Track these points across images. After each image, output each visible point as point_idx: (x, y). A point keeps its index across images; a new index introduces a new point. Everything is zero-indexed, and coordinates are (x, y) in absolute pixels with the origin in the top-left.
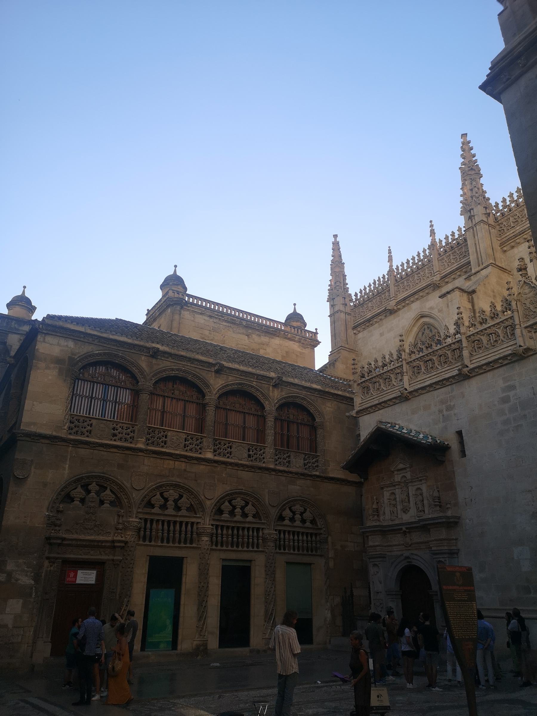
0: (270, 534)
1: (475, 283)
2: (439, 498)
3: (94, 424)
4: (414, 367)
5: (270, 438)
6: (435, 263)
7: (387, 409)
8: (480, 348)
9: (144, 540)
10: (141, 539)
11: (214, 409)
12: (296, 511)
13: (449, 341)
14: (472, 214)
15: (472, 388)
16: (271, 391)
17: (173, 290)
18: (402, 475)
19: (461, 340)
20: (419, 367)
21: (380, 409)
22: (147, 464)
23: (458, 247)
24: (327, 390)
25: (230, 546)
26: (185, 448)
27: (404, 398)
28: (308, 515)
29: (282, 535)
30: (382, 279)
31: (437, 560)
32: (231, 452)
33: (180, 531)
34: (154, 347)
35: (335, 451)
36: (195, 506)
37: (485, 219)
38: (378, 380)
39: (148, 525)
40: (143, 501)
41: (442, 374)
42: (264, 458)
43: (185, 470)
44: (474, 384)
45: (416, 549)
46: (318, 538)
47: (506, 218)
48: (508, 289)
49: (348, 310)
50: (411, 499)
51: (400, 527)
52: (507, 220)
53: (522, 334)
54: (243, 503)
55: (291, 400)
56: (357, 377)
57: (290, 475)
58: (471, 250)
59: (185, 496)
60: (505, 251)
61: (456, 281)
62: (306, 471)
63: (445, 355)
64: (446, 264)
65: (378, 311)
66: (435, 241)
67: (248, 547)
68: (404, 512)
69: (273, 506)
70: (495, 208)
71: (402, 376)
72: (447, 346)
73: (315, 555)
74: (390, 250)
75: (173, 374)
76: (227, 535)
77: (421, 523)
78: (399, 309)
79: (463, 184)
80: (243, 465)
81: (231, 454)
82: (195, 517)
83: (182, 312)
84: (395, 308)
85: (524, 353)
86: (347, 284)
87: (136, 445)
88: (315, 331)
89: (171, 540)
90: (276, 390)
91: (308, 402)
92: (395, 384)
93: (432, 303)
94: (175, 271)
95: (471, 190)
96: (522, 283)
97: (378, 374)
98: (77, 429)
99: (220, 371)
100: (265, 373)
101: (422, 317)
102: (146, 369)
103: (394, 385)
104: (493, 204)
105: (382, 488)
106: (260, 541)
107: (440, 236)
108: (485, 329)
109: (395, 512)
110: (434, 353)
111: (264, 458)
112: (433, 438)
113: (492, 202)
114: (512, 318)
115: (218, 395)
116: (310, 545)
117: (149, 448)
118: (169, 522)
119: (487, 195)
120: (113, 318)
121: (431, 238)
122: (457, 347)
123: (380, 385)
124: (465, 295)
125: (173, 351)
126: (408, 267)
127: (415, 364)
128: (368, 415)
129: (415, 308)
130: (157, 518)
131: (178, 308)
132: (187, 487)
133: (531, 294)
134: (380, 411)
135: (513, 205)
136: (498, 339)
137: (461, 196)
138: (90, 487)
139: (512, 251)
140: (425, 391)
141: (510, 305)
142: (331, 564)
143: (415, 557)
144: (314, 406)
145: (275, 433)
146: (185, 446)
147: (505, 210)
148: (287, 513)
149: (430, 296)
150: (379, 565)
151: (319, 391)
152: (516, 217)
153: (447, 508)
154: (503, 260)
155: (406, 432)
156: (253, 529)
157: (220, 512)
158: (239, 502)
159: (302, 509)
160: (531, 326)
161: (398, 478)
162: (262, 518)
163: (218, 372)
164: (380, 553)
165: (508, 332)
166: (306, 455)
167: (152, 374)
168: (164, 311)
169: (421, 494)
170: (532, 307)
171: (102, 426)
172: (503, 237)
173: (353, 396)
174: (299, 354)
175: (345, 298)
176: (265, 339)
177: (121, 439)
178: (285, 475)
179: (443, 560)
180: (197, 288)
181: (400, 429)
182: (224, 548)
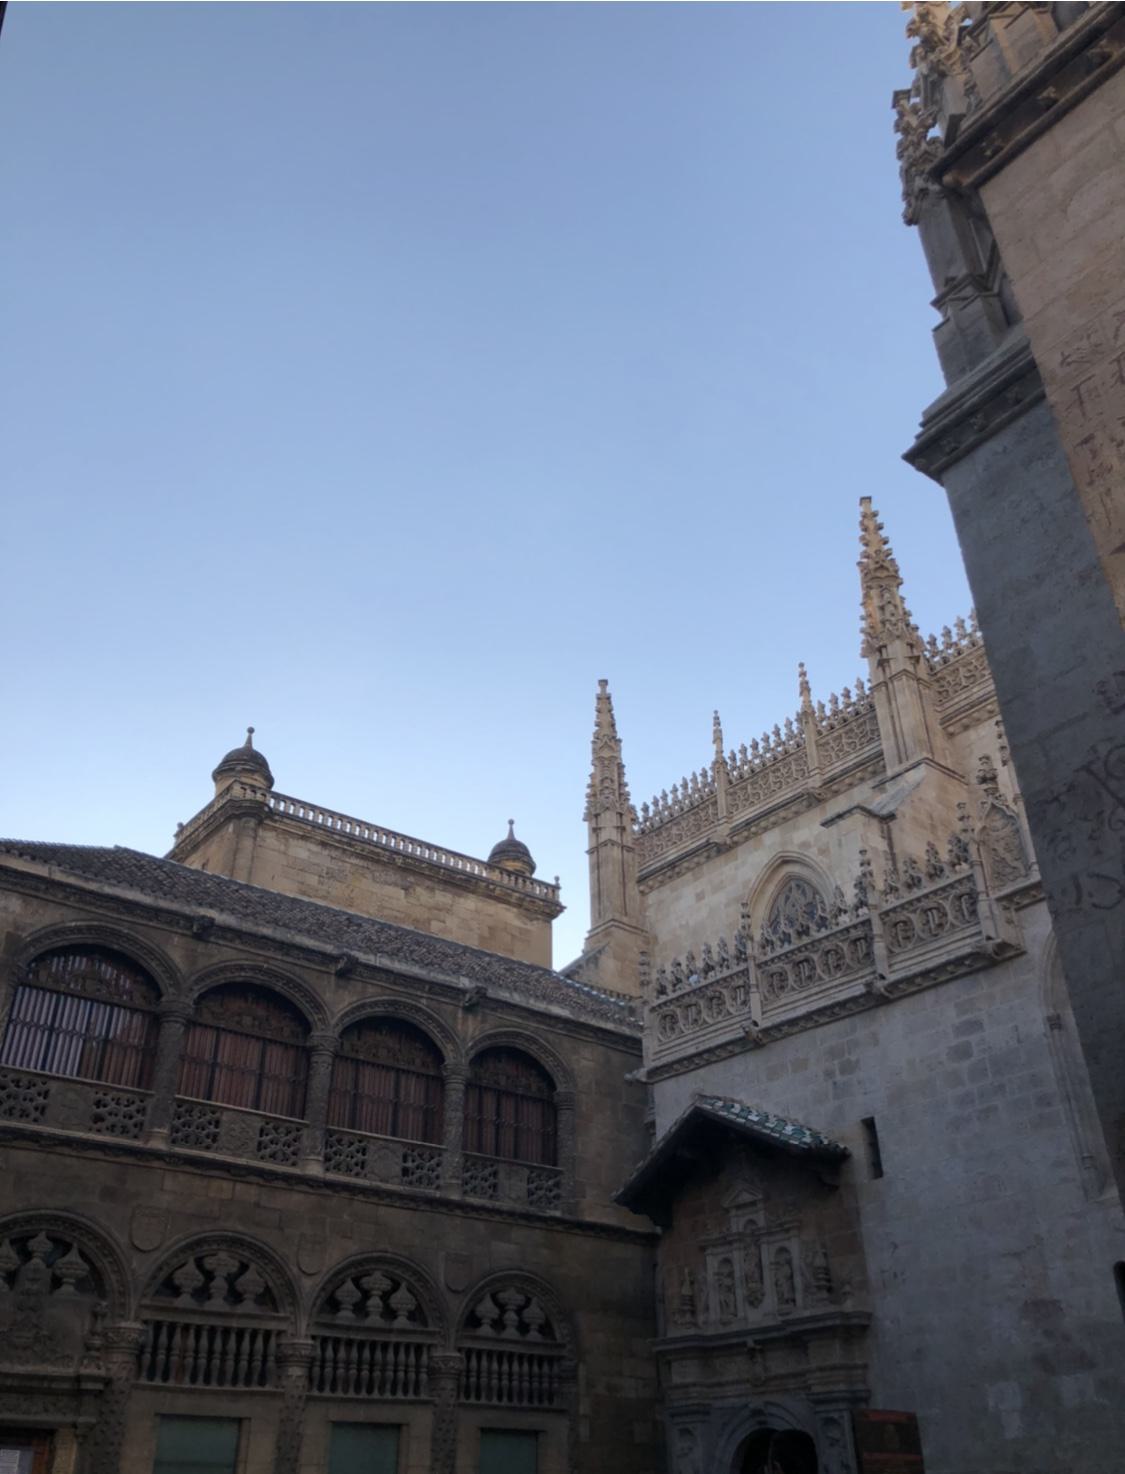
0: (446, 1360)
1: (893, 797)
2: (827, 1270)
3: (52, 1091)
4: (772, 976)
5: (453, 1131)
6: (812, 750)
9: (151, 1377)
10: (144, 1374)
11: (330, 1061)
12: (506, 1304)
13: (845, 920)
14: (885, 656)
15: (893, 1022)
16: (460, 1021)
17: (242, 783)
20: (782, 975)
21: (699, 1067)
22: (170, 1190)
23: (856, 721)
24: (582, 1020)
25: (352, 1390)
26: (259, 1150)
27: (751, 1043)
28: (534, 1313)
29: (474, 1363)
30: (700, 779)
32: (363, 1163)
33: (238, 1354)
34: (203, 917)
35: (599, 1161)
36: (275, 1292)
37: (910, 668)
38: (694, 1000)
39: (163, 1339)
40: (154, 1277)
41: (832, 991)
42: (438, 1177)
43: (257, 1205)
46: (556, 1369)
47: (951, 668)
48: (961, 819)
49: (628, 840)
50: (767, 1274)
51: (741, 1340)
52: (954, 671)
53: (992, 912)
54: (386, 1284)
55: (503, 1041)
56: (649, 994)
57: (497, 1218)
58: (885, 727)
59: (253, 1266)
60: (951, 735)
61: (856, 790)
62: (532, 1210)
63: (837, 951)
64: (833, 754)
65: (693, 846)
66: (810, 706)
67: (394, 1392)
68: (751, 1303)
69: (454, 1292)
70: (928, 647)
71: (747, 993)
72: (841, 931)
73: (547, 1411)
74: (717, 718)
75: (241, 976)
76: (348, 1363)
77: (790, 1329)
78: (736, 844)
79: (866, 596)
80: (390, 1194)
81: (362, 1168)
82: (274, 1318)
83: (261, 832)
84: (728, 841)
85: (997, 954)
86: (626, 785)
87: (147, 1141)
88: (553, 882)
89: (215, 1374)
90: (470, 1017)
91: (542, 1047)
92: (732, 1010)
93: (807, 832)
94: (249, 741)
95: (882, 608)
96: (988, 807)
97: (695, 986)
98: (12, 1102)
99: (349, 971)
100: (448, 978)
101: (786, 862)
102: (181, 966)
103: (729, 1013)
104: (926, 639)
105: (703, 1249)
106: (424, 1377)
107: (820, 696)
108: (918, 900)
110: (813, 946)
111: (438, 1177)
112: (815, 1135)
113: (924, 634)
114: (970, 878)
115: (340, 1028)
116: (536, 1385)
117: (178, 1150)
118: (212, 1330)
119: (913, 621)
120: (109, 844)
121: (802, 699)
122: (862, 937)
123: (699, 1012)
124: (875, 823)
125: (247, 926)
126: (755, 756)
127: (774, 968)
128: (674, 1079)
129: (772, 842)
130: (182, 1320)
131: (252, 823)
132: (260, 1245)
134: (701, 1072)
135: (964, 642)
136: (943, 920)
137: (862, 618)
138: (32, 1244)
139: (965, 734)
140: (796, 1029)
141: (966, 850)
142: (584, 1431)
143: (774, 1410)
144: (553, 1055)
145: (466, 1118)
146: (260, 1146)
147: (950, 651)
148: (487, 1309)
149: (801, 819)
151: (566, 1021)
152: (971, 667)
153: (845, 1294)
154: (947, 752)
155: (756, 1119)
156: (408, 1347)
157: (333, 1304)
158: (377, 1282)
159: (520, 1299)
160: (1009, 897)
161: (737, 1224)
162: (430, 1321)
163: (343, 975)
164: (696, 1402)
165: (964, 906)
166: (532, 1169)
167: (193, 978)
168: (218, 829)
169: (789, 1262)
170: (1008, 857)
171: (71, 1095)
172: (948, 705)
173: (640, 1035)
174: (517, 934)
175: (621, 815)
176: (442, 897)
177: (112, 1129)
178: (485, 1216)
179: (836, 1416)
180: (297, 778)
181: (743, 1114)
182: (340, 1394)
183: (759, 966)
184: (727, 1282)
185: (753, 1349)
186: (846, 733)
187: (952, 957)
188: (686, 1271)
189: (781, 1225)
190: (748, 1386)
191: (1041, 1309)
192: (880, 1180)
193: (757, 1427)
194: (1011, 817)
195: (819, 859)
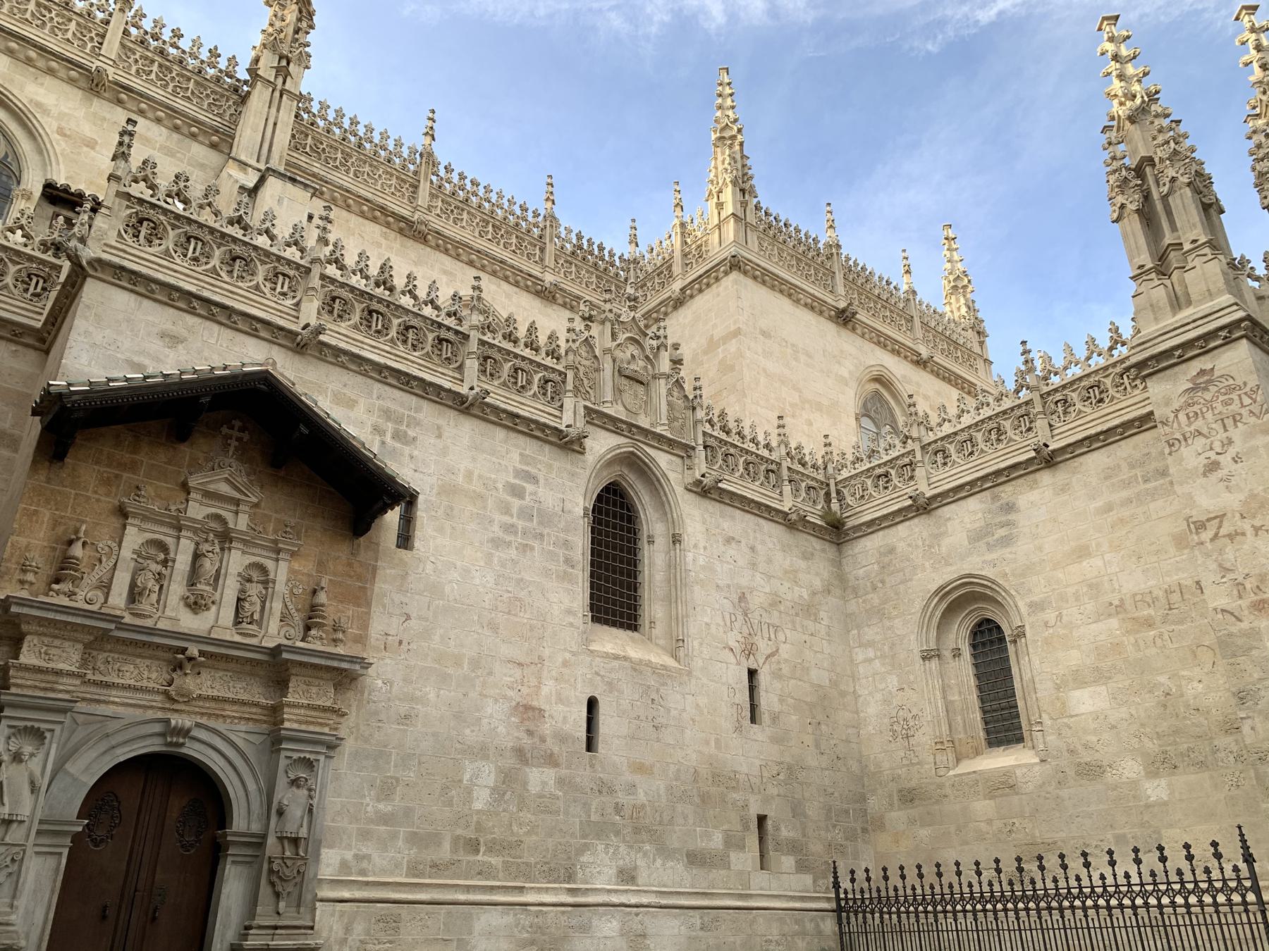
4: (334, 299)
7: (216, 327)
8: (491, 375)
18: (213, 510)
19: (466, 337)
21: (192, 312)
31: (289, 754)
38: (208, 237)
44: (464, 430)
52: (302, 132)
103: (257, 288)
105: (122, 513)
108: (516, 356)
109: (154, 597)
128: (133, 296)
133: (587, 363)
149: (48, 80)
153: (334, 640)
161: (197, 510)
164: (60, 696)
179: (312, 757)
183: (323, 277)
184: (155, 567)
185: (190, 659)
186: (160, 66)
187: (543, 420)
188: (84, 528)
189: (276, 542)
190: (159, 698)
191: (528, 712)
192: (403, 553)
193: (164, 749)
194: (596, 357)
195: (55, 137)
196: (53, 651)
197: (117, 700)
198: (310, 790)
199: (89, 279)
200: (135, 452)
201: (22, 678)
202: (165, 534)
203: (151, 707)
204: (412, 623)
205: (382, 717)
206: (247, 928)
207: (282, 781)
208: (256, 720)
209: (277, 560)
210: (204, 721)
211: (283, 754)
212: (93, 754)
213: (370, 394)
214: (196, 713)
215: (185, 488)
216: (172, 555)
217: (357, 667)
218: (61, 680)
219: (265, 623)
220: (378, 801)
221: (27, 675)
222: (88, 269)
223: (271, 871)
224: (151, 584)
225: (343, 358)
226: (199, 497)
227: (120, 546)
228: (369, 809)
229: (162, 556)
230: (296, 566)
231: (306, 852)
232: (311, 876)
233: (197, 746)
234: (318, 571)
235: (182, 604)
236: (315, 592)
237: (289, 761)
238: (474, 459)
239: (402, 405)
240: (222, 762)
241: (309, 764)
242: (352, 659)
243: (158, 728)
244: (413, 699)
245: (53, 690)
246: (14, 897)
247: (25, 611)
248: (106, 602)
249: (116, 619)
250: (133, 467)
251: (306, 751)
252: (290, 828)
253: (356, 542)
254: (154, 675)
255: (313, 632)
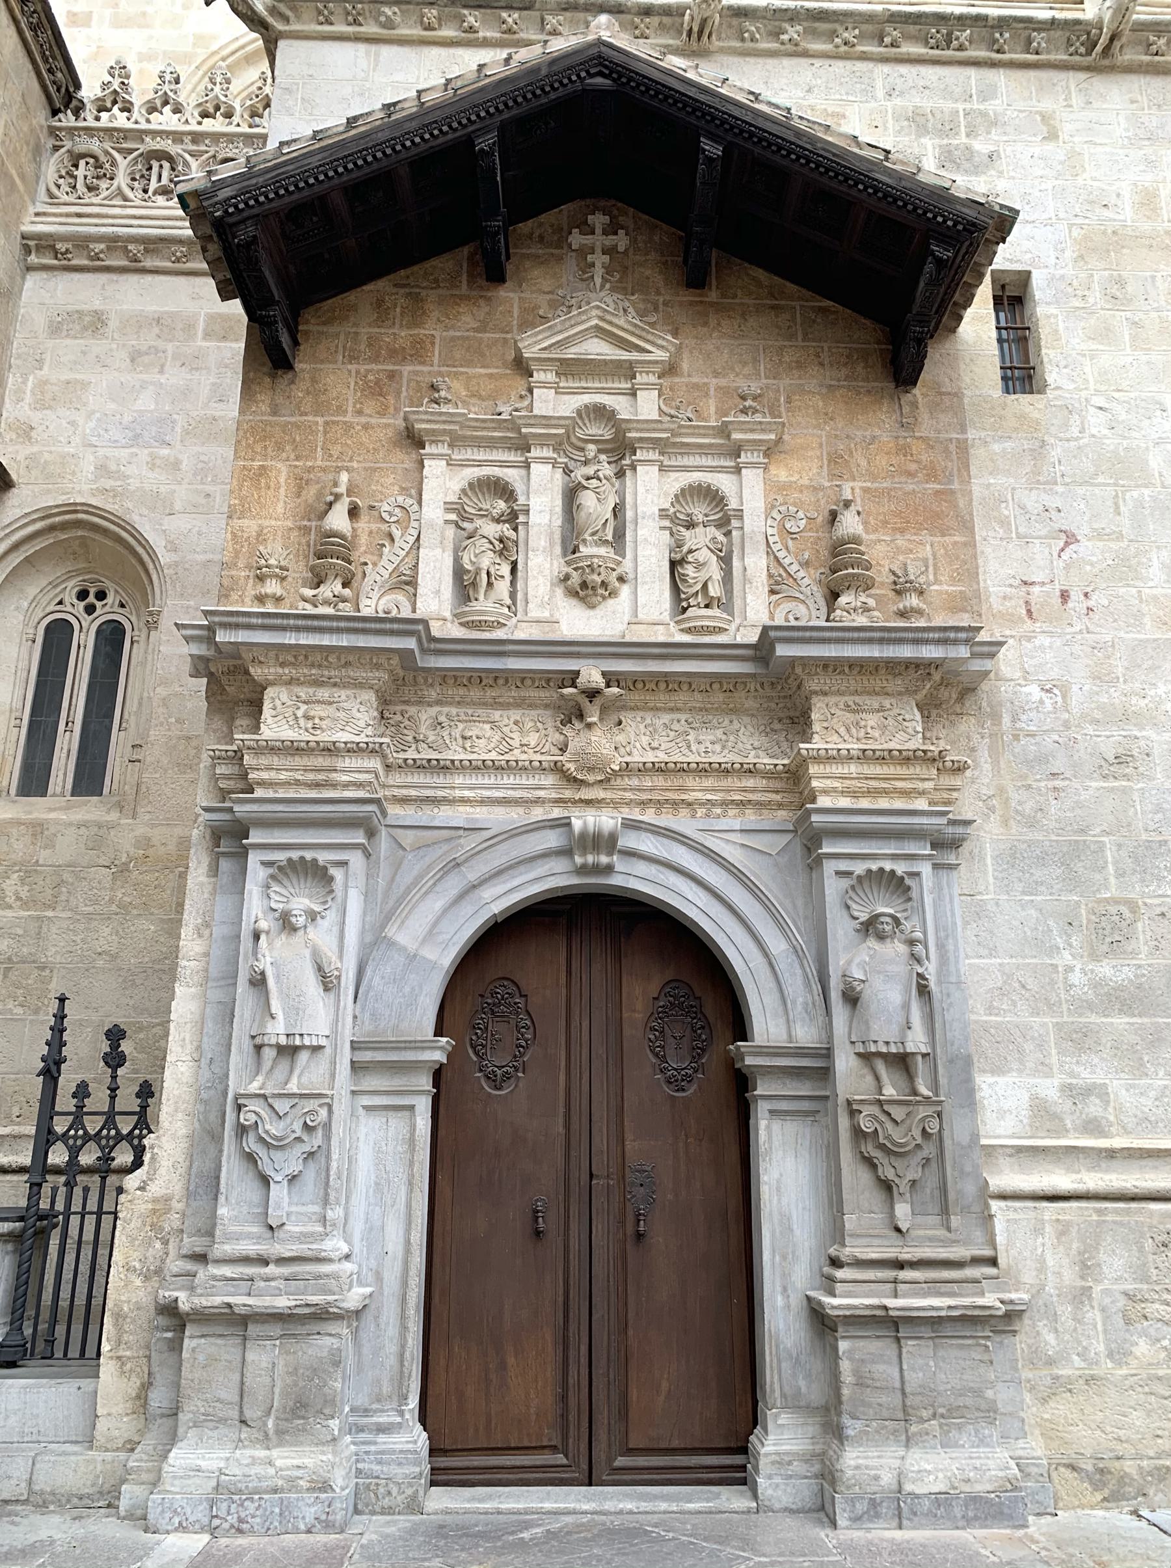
18: (587, 399)
31: (843, 866)
45: (643, 804)
77: (782, 650)
105: (414, 440)
109: (502, 588)
128: (362, 47)
150: (332, 871)
153: (902, 614)
169: (723, 523)
179: (900, 868)
184: (491, 530)
185: (592, 694)
188: (344, 477)
189: (724, 431)
190: (549, 780)
193: (575, 880)
196: (318, 711)
197: (467, 793)
198: (911, 943)
199: (282, 44)
200: (416, 322)
201: (269, 768)
202: (503, 464)
203: (538, 801)
204: (1085, 548)
205: (1058, 765)
206: (835, 1263)
207: (840, 930)
208: (760, 805)
209: (738, 470)
210: (649, 816)
211: (830, 867)
212: (436, 903)
213: (869, 92)
214: (629, 803)
215: (522, 367)
216: (522, 500)
217: (963, 652)
218: (340, 764)
219: (737, 603)
220: (1095, 957)
221: (276, 761)
222: (270, 20)
223: (858, 1133)
224: (487, 561)
225: (793, 32)
226: (551, 377)
227: (420, 503)
228: (1076, 978)
229: (501, 505)
230: (781, 474)
231: (935, 1087)
232: (965, 1140)
233: (642, 868)
234: (832, 476)
235: (559, 592)
236: (833, 516)
237: (845, 883)
238: (1151, 164)
239: (946, 93)
240: (701, 898)
241: (897, 885)
242: (945, 636)
243: (552, 839)
244: (1126, 717)
245: (334, 785)
246: (326, 1202)
247: (242, 636)
248: (414, 611)
249: (416, 627)
250: (418, 352)
251: (884, 856)
252: (883, 1035)
253: (906, 398)
254: (533, 739)
255: (843, 600)
